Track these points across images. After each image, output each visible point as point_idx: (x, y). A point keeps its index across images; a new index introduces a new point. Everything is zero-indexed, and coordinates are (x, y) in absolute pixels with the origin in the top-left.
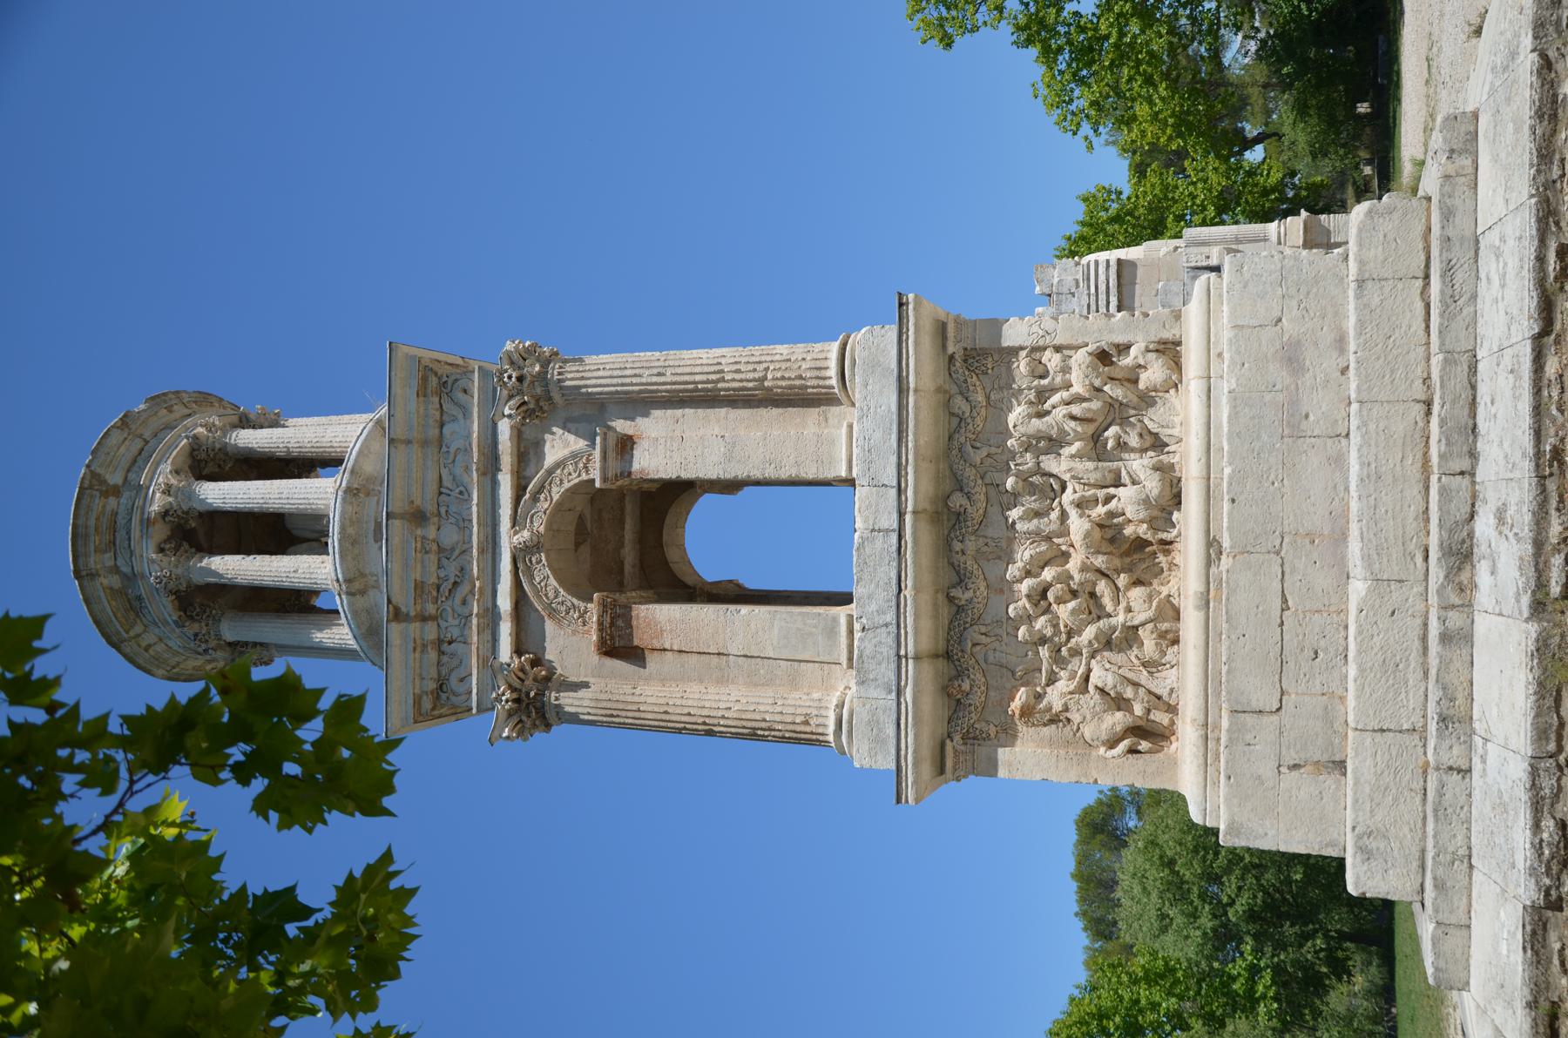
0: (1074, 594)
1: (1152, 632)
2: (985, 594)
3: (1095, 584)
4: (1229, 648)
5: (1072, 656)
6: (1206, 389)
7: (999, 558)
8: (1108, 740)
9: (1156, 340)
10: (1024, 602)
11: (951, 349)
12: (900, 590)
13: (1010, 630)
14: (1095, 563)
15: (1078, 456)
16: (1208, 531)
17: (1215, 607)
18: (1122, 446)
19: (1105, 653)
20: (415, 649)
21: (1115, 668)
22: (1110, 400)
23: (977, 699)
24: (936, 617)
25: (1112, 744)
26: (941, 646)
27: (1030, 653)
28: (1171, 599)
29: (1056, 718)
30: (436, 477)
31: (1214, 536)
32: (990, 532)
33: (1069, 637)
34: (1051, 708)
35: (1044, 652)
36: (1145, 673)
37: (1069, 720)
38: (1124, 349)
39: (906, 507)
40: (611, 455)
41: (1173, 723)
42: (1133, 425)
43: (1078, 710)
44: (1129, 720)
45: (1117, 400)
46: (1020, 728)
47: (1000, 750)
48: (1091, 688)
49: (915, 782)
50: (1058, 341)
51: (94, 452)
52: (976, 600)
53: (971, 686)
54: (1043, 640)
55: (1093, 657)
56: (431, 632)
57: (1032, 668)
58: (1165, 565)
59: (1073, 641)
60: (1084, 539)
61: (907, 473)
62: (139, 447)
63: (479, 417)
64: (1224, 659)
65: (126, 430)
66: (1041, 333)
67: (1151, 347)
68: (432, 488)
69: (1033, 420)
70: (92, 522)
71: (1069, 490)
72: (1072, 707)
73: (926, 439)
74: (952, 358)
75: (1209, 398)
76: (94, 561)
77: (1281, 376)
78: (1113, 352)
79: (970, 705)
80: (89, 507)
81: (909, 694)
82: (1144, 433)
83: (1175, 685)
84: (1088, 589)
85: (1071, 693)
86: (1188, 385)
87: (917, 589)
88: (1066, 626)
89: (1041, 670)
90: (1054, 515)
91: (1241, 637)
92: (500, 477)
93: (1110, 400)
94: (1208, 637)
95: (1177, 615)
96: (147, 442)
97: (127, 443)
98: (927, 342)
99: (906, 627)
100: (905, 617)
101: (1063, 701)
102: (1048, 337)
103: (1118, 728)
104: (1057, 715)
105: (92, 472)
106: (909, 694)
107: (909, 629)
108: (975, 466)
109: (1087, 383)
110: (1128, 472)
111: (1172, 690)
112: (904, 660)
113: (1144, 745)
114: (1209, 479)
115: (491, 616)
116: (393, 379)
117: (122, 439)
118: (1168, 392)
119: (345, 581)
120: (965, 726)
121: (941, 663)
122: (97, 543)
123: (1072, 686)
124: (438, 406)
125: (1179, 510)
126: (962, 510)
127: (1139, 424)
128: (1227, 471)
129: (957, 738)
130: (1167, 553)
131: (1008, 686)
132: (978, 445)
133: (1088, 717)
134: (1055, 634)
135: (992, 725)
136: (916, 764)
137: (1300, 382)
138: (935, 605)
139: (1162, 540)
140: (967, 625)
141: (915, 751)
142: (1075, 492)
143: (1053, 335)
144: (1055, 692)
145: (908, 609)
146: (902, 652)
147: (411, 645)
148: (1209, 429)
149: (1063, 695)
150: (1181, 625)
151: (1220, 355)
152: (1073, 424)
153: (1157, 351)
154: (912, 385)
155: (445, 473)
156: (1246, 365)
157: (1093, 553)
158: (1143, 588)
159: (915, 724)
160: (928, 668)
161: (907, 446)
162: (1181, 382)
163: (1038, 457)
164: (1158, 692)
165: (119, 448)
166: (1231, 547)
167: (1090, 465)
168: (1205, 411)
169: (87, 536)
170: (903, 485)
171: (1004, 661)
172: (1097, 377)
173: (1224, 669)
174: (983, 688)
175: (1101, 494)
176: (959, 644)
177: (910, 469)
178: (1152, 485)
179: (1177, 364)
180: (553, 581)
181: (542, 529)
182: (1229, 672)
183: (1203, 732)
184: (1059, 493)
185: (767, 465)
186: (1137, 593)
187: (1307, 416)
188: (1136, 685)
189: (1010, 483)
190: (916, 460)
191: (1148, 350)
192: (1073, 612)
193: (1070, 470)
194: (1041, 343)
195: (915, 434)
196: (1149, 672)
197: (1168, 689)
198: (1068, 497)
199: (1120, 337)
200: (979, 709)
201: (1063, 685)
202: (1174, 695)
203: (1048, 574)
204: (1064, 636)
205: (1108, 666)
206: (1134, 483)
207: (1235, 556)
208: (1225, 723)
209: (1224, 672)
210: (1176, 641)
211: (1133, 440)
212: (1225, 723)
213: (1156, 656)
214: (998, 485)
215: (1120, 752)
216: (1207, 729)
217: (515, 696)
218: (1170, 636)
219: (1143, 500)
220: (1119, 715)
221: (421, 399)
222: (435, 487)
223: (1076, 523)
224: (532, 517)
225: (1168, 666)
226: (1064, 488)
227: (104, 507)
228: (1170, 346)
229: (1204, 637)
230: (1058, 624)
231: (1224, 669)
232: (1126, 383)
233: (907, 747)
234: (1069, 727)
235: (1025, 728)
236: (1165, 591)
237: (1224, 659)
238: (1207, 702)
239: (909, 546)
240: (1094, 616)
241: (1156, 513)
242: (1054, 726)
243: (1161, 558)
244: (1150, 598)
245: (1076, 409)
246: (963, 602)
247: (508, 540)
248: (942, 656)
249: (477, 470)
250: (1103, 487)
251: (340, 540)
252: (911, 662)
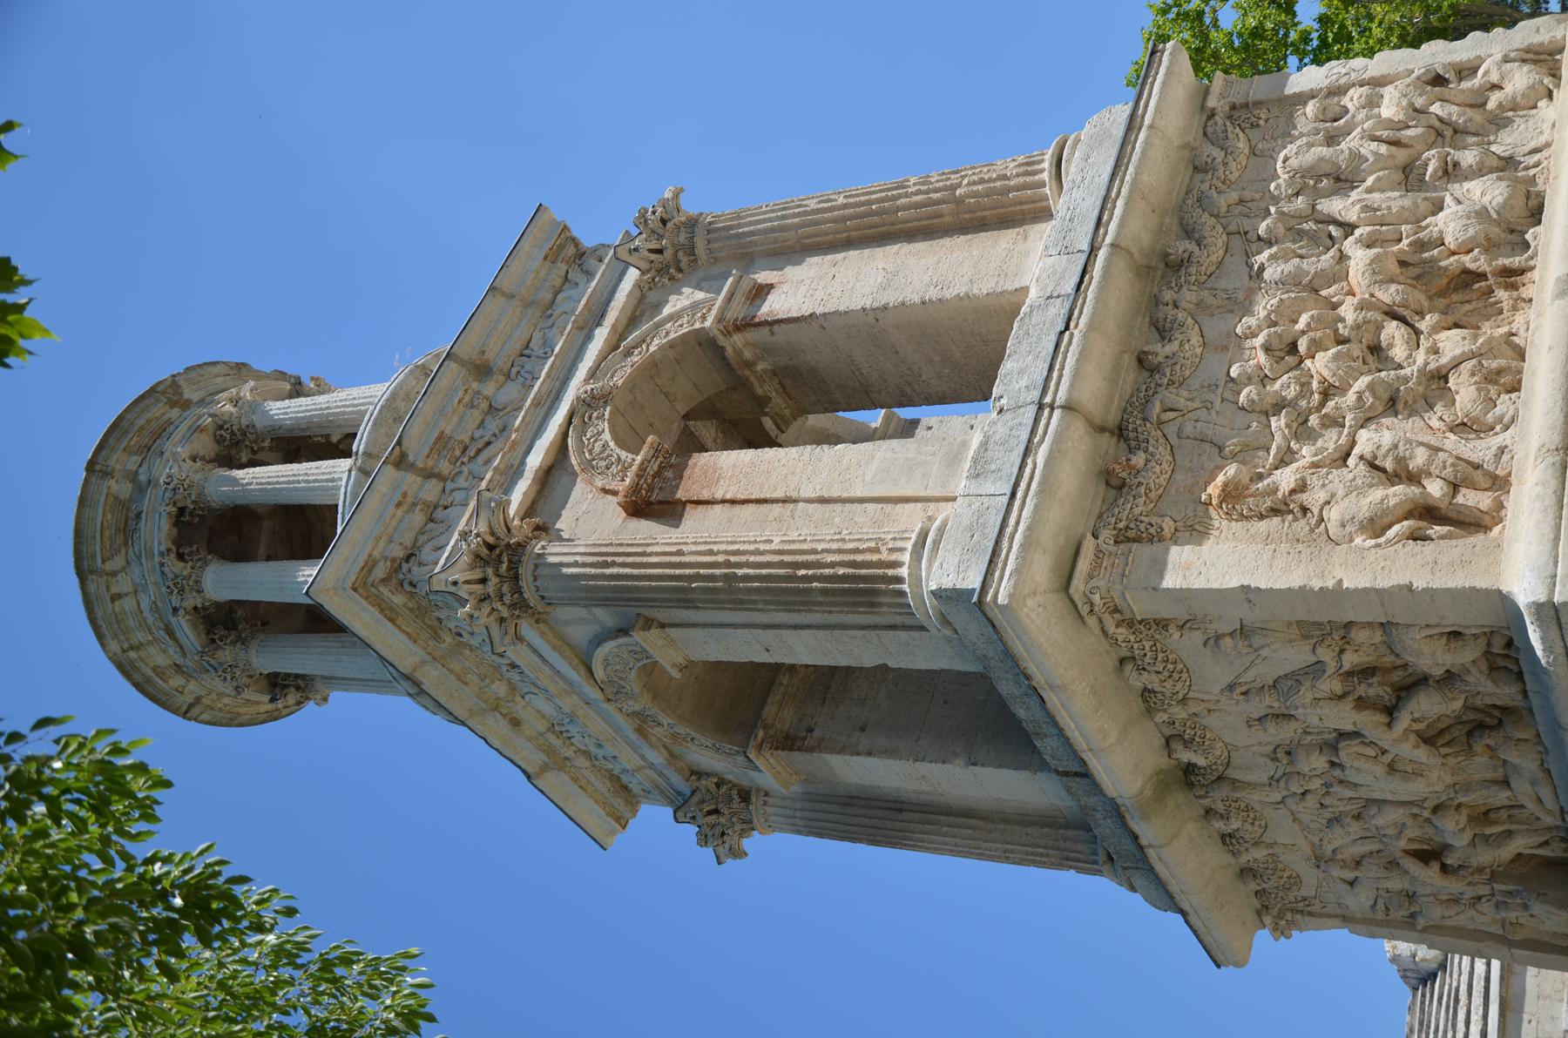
1: (1473, 374)
2: (1199, 351)
3: (1380, 328)
5: (1324, 426)
7: (1232, 311)
8: (1371, 520)
10: (1262, 357)
11: (1212, 102)
13: (1228, 395)
19: (1384, 420)
20: (399, 505)
22: (1437, 124)
23: (1156, 476)
24: (1113, 378)
26: (1113, 418)
27: (1255, 424)
29: (1283, 507)
30: (525, 337)
32: (1223, 283)
33: (1326, 395)
34: (1277, 489)
35: (1278, 423)
37: (1305, 510)
39: (1103, 241)
40: (740, 298)
41: (1500, 506)
46: (1216, 524)
49: (1017, 571)
52: (1182, 354)
53: (1147, 461)
54: (1279, 406)
56: (431, 490)
57: (1256, 444)
58: (1506, 305)
59: (1331, 404)
60: (1370, 264)
61: (1114, 207)
63: (602, 275)
67: (1513, 55)
68: (516, 345)
70: (141, 422)
74: (1212, 114)
79: (1140, 484)
80: (148, 407)
81: (1041, 455)
84: (1367, 338)
89: (1268, 450)
93: (1437, 124)
99: (1062, 369)
106: (1041, 455)
107: (1067, 372)
108: (1217, 216)
109: (1404, 103)
112: (1047, 411)
115: (516, 472)
116: (526, 235)
118: (1535, 107)
121: (1107, 442)
122: (132, 443)
124: (563, 274)
129: (1107, 534)
131: (1210, 466)
133: (1341, 493)
134: (1300, 396)
135: (1167, 519)
136: (1025, 546)
138: (1116, 367)
141: (1030, 528)
147: (398, 497)
150: (1526, 365)
155: (537, 337)
157: (1382, 282)
159: (1040, 492)
160: (1081, 440)
169: (126, 432)
170: (1105, 218)
171: (1210, 433)
172: (1421, 95)
174: (1165, 465)
176: (1142, 411)
177: (1120, 203)
181: (620, 382)
185: (932, 287)
190: (1131, 192)
191: (1506, 60)
195: (1138, 168)
200: (1153, 495)
202: (1505, 457)
213: (1477, 412)
214: (1246, 233)
219: (1476, 212)
221: (548, 263)
225: (1498, 428)
227: (163, 414)
230: (1310, 383)
233: (1018, 523)
234: (1303, 522)
241: (1495, 231)
242: (1276, 520)
243: (1502, 294)
246: (1160, 359)
248: (1112, 433)
249: (573, 322)
251: (382, 407)
252: (1057, 413)
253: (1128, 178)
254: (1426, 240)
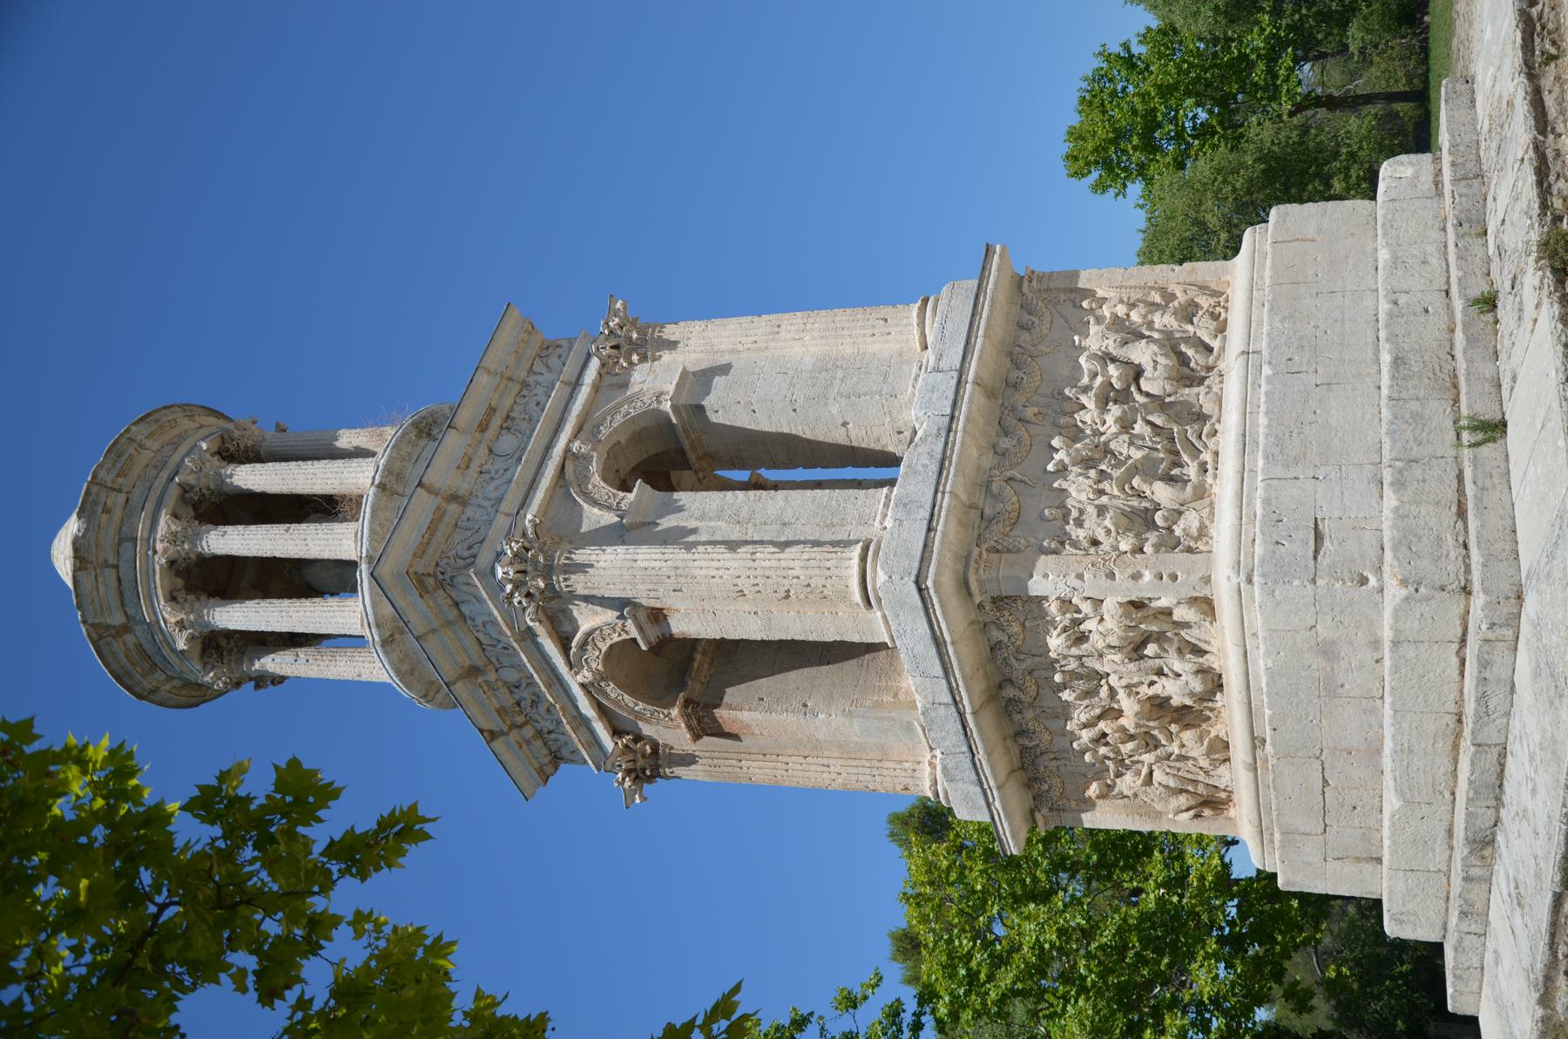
6: (1242, 652)
12: (973, 755)
16: (1252, 732)
17: (1262, 774)
20: (520, 747)
30: (473, 641)
40: (647, 627)
42: (1169, 640)
47: (1083, 816)
51: (79, 606)
56: (528, 732)
62: (114, 577)
63: (495, 606)
65: (89, 566)
68: (474, 650)
70: (124, 661)
75: (1246, 657)
76: (148, 683)
77: (1318, 662)
80: (112, 652)
82: (1183, 644)
87: (989, 754)
90: (1104, 692)
92: (540, 640)
96: (116, 567)
97: (99, 579)
98: (954, 603)
100: (983, 771)
105: (91, 625)
106: (997, 804)
113: (1207, 812)
114: (1250, 703)
115: (582, 722)
116: (392, 599)
117: (93, 578)
119: (367, 556)
122: (140, 671)
125: (1222, 691)
127: (1176, 639)
128: (1268, 712)
132: (1022, 657)
137: (1335, 667)
147: (517, 747)
154: (948, 639)
155: (480, 635)
158: (1193, 730)
165: (98, 590)
168: (1242, 665)
169: (127, 672)
180: (626, 696)
182: (1278, 815)
187: (1342, 686)
188: (1195, 782)
189: (1058, 678)
205: (1168, 770)
217: (633, 776)
221: (426, 596)
222: (477, 648)
224: (586, 660)
227: (125, 644)
232: (1160, 616)
236: (1213, 734)
239: (974, 731)
240: (1151, 746)
244: (1201, 739)
247: (574, 683)
249: (515, 641)
251: (400, 680)
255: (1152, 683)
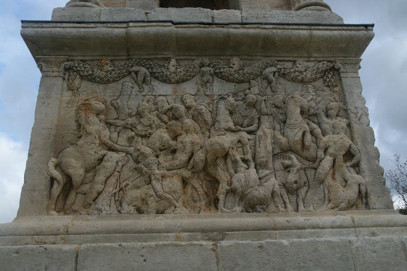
0: (175, 138)
1: (146, 194)
4: (134, 248)
9: (369, 191)
14: (199, 152)
15: (275, 142)
18: (287, 168)
21: (118, 169)
25: (58, 166)
28: (173, 208)
29: (82, 128)
31: (227, 235)
36: (114, 191)
38: (356, 166)
43: (87, 142)
44: (77, 179)
45: (319, 166)
48: (105, 152)
50: (355, 126)
55: (127, 153)
64: (124, 244)
66: (359, 114)
69: (299, 109)
71: (250, 137)
72: (89, 139)
73: (278, 43)
78: (354, 161)
83: (104, 212)
85: (100, 137)
86: (341, 215)
88: (150, 134)
91: (143, 259)
94: (143, 232)
95: (160, 212)
101: (93, 132)
102: (357, 119)
103: (71, 171)
104: (84, 128)
109: (330, 144)
110: (267, 175)
111: (100, 210)
113: (57, 189)
120: (79, 68)
123: (106, 140)
126: (232, 65)
128: (285, 242)
130: (208, 205)
139: (218, 200)
140: (150, 70)
142: (249, 140)
143: (358, 122)
144: (101, 128)
145: (162, 28)
146: (131, 24)
148: (313, 228)
149: (99, 132)
150: (152, 215)
151: (373, 234)
152: (300, 134)
153: (360, 192)
156: (374, 254)
161: (273, 28)
162: (340, 210)
163: (272, 115)
164: (100, 200)
166: (222, 247)
167: (270, 148)
170: (247, 26)
173: (115, 245)
175: (249, 156)
178: (261, 192)
179: (351, 206)
182: (112, 248)
183: (61, 231)
184: (247, 129)
186: (177, 183)
192: (162, 137)
193: (265, 134)
194: (352, 115)
196: (115, 193)
197: (101, 207)
198: (245, 135)
199: (365, 166)
201: (106, 133)
202: (96, 212)
203: (188, 121)
204: (143, 133)
205: (120, 164)
206: (260, 179)
207: (214, 250)
208: (67, 247)
209: (114, 245)
210: (139, 211)
211: (292, 177)
212: (67, 247)
215: (52, 172)
216: (65, 234)
218: (143, 208)
220: (82, 171)
223: (227, 139)
225: (119, 208)
226: (250, 133)
228: (364, 200)
229: (143, 229)
231: (115, 245)
232: (331, 171)
235: (75, 108)
236: (178, 204)
237: (124, 244)
238: (88, 233)
245: (309, 137)
250: (254, 159)
252: (125, 30)
253: (274, 31)
254: (238, 165)
255: (245, 161)
